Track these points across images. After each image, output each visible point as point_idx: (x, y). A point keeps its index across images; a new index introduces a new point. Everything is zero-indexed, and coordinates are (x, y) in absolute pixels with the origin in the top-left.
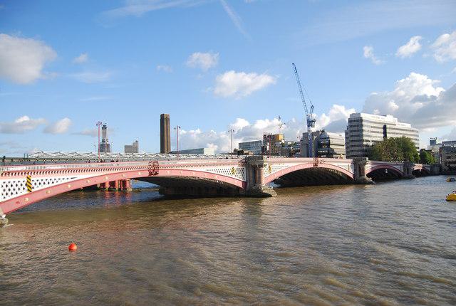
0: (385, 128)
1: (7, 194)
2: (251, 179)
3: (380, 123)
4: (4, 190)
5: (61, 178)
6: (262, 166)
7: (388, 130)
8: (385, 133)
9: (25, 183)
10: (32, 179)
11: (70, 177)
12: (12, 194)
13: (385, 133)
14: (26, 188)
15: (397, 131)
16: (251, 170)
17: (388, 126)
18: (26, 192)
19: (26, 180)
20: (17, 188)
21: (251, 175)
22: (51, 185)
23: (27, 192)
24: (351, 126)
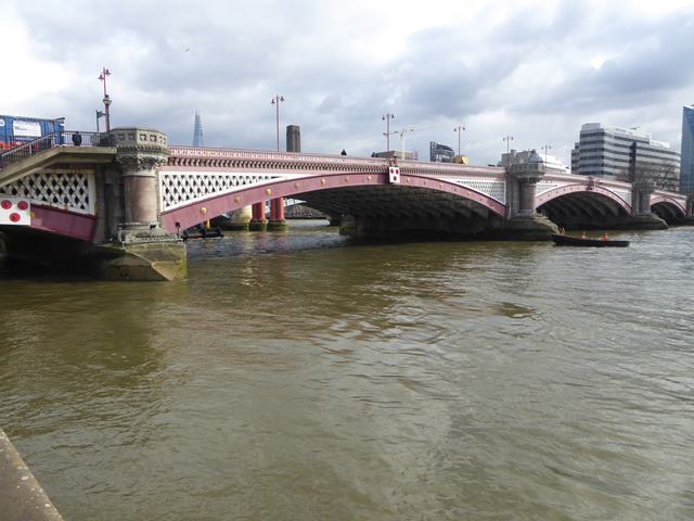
0: (633, 147)
1: (172, 198)
2: (516, 202)
3: (630, 140)
4: (167, 191)
5: (257, 175)
6: (535, 180)
7: (638, 151)
8: (633, 155)
11: (270, 175)
12: (180, 198)
13: (633, 155)
15: (657, 154)
16: (516, 188)
17: (639, 144)
20: (187, 189)
21: (516, 195)
24: (583, 143)
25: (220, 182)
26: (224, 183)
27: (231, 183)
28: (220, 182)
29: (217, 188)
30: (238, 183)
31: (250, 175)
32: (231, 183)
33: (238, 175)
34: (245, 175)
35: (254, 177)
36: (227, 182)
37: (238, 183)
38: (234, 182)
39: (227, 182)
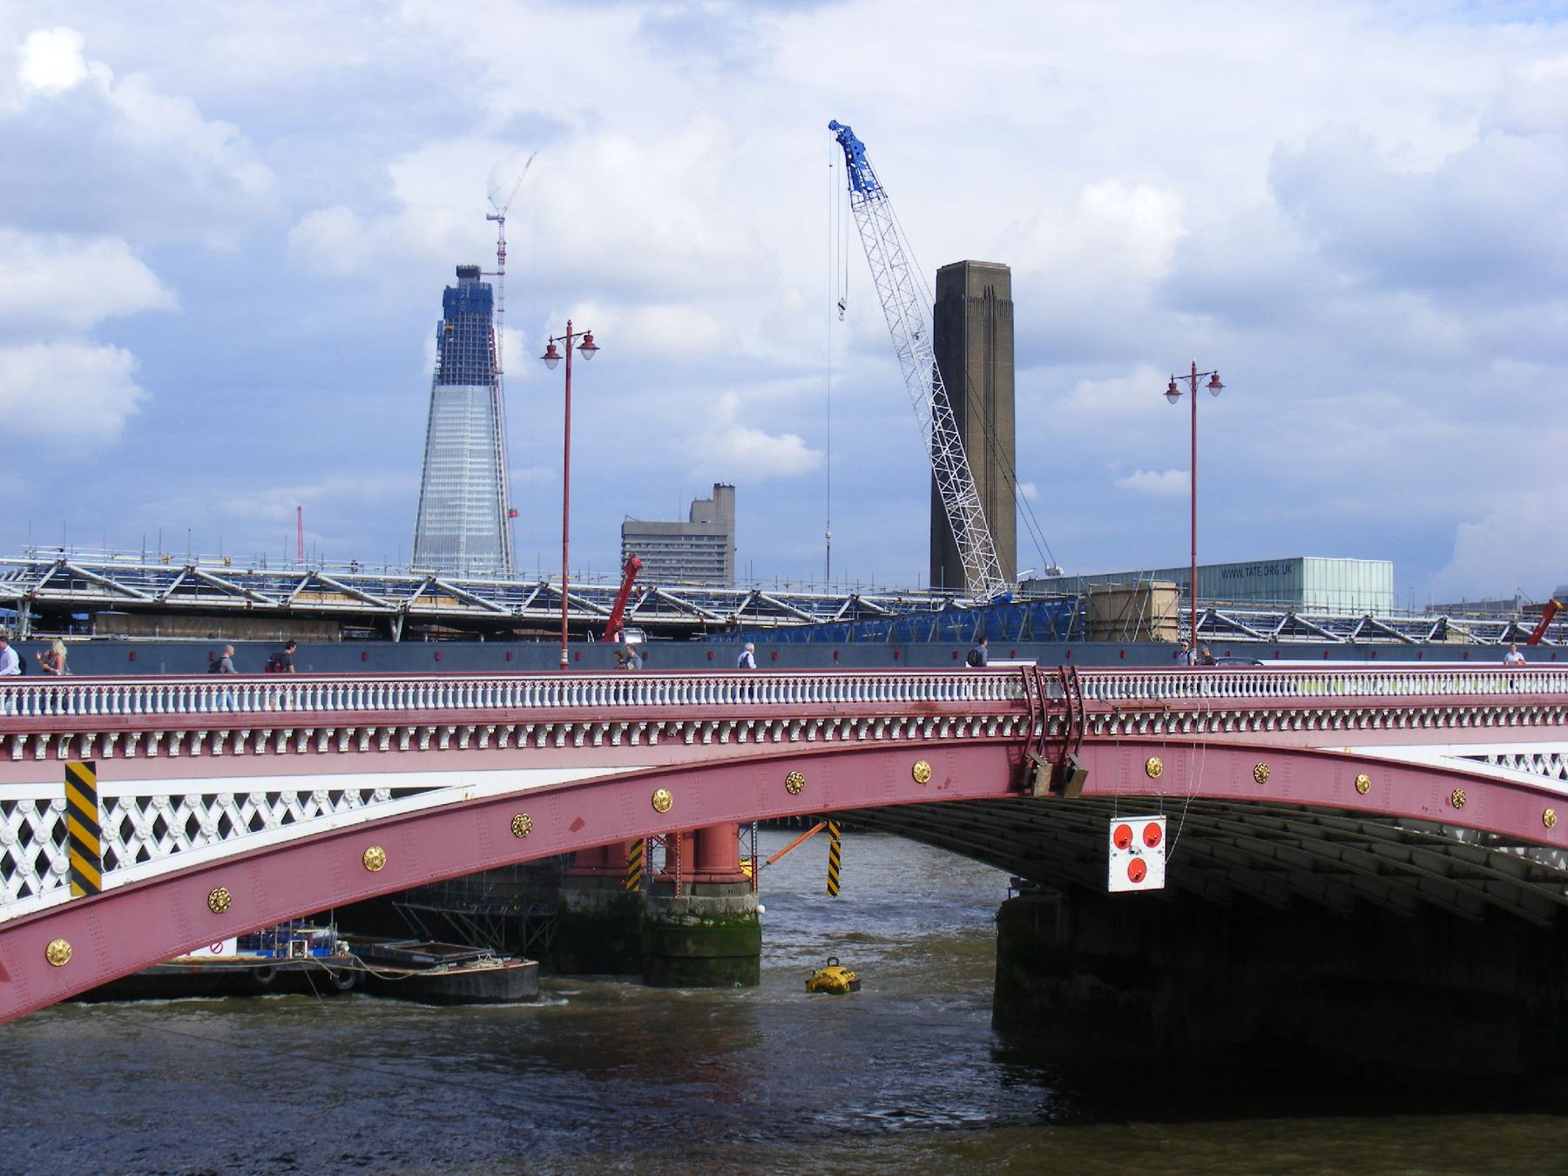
5: (320, 784)
9: (51, 819)
10: (103, 790)
11: (381, 782)
14: (60, 858)
18: (52, 893)
19: (57, 792)
22: (242, 842)
23: (64, 895)
25: (144, 823)
26: (160, 829)
27: (192, 827)
28: (144, 823)
30: (225, 826)
31: (288, 786)
32: (192, 827)
33: (226, 788)
34: (258, 787)
35: (304, 797)
36: (177, 821)
37: (225, 826)
38: (209, 820)
39: (177, 821)
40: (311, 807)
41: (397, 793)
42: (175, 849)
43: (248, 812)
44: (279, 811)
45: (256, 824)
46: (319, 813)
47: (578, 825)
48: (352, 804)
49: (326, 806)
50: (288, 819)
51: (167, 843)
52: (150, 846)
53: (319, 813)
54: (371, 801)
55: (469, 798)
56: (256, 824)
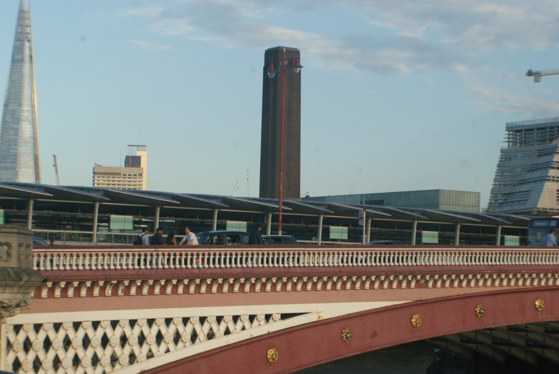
5: (244, 311)
11: (276, 309)
25: (151, 334)
26: (160, 337)
27: (177, 338)
28: (151, 334)
29: (141, 352)
30: (194, 337)
31: (228, 311)
35: (236, 319)
36: (169, 333)
37: (194, 337)
38: (186, 332)
39: (169, 333)
40: (239, 324)
41: (284, 316)
42: (168, 351)
43: (223, 326)
44: (223, 326)
45: (211, 336)
46: (244, 328)
47: (374, 335)
48: (261, 323)
49: (247, 324)
50: (227, 332)
51: (163, 346)
52: (154, 348)
53: (244, 328)
54: (271, 320)
55: (320, 319)
56: (211, 336)
